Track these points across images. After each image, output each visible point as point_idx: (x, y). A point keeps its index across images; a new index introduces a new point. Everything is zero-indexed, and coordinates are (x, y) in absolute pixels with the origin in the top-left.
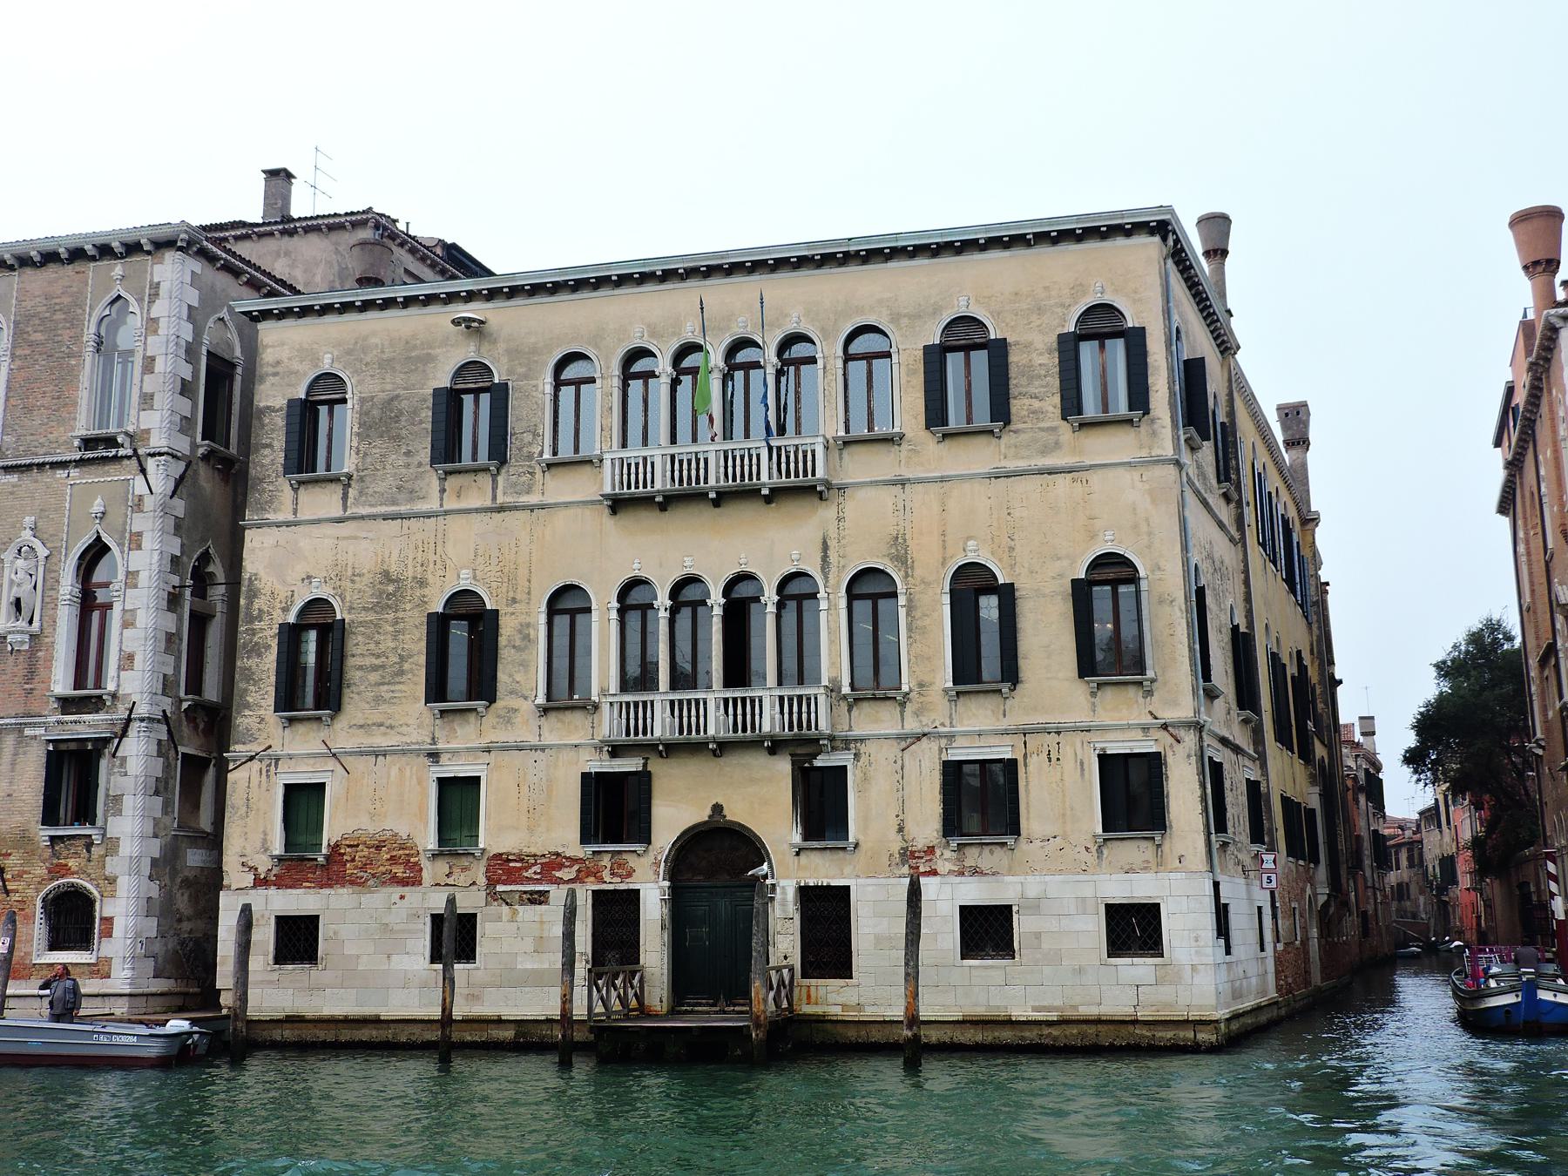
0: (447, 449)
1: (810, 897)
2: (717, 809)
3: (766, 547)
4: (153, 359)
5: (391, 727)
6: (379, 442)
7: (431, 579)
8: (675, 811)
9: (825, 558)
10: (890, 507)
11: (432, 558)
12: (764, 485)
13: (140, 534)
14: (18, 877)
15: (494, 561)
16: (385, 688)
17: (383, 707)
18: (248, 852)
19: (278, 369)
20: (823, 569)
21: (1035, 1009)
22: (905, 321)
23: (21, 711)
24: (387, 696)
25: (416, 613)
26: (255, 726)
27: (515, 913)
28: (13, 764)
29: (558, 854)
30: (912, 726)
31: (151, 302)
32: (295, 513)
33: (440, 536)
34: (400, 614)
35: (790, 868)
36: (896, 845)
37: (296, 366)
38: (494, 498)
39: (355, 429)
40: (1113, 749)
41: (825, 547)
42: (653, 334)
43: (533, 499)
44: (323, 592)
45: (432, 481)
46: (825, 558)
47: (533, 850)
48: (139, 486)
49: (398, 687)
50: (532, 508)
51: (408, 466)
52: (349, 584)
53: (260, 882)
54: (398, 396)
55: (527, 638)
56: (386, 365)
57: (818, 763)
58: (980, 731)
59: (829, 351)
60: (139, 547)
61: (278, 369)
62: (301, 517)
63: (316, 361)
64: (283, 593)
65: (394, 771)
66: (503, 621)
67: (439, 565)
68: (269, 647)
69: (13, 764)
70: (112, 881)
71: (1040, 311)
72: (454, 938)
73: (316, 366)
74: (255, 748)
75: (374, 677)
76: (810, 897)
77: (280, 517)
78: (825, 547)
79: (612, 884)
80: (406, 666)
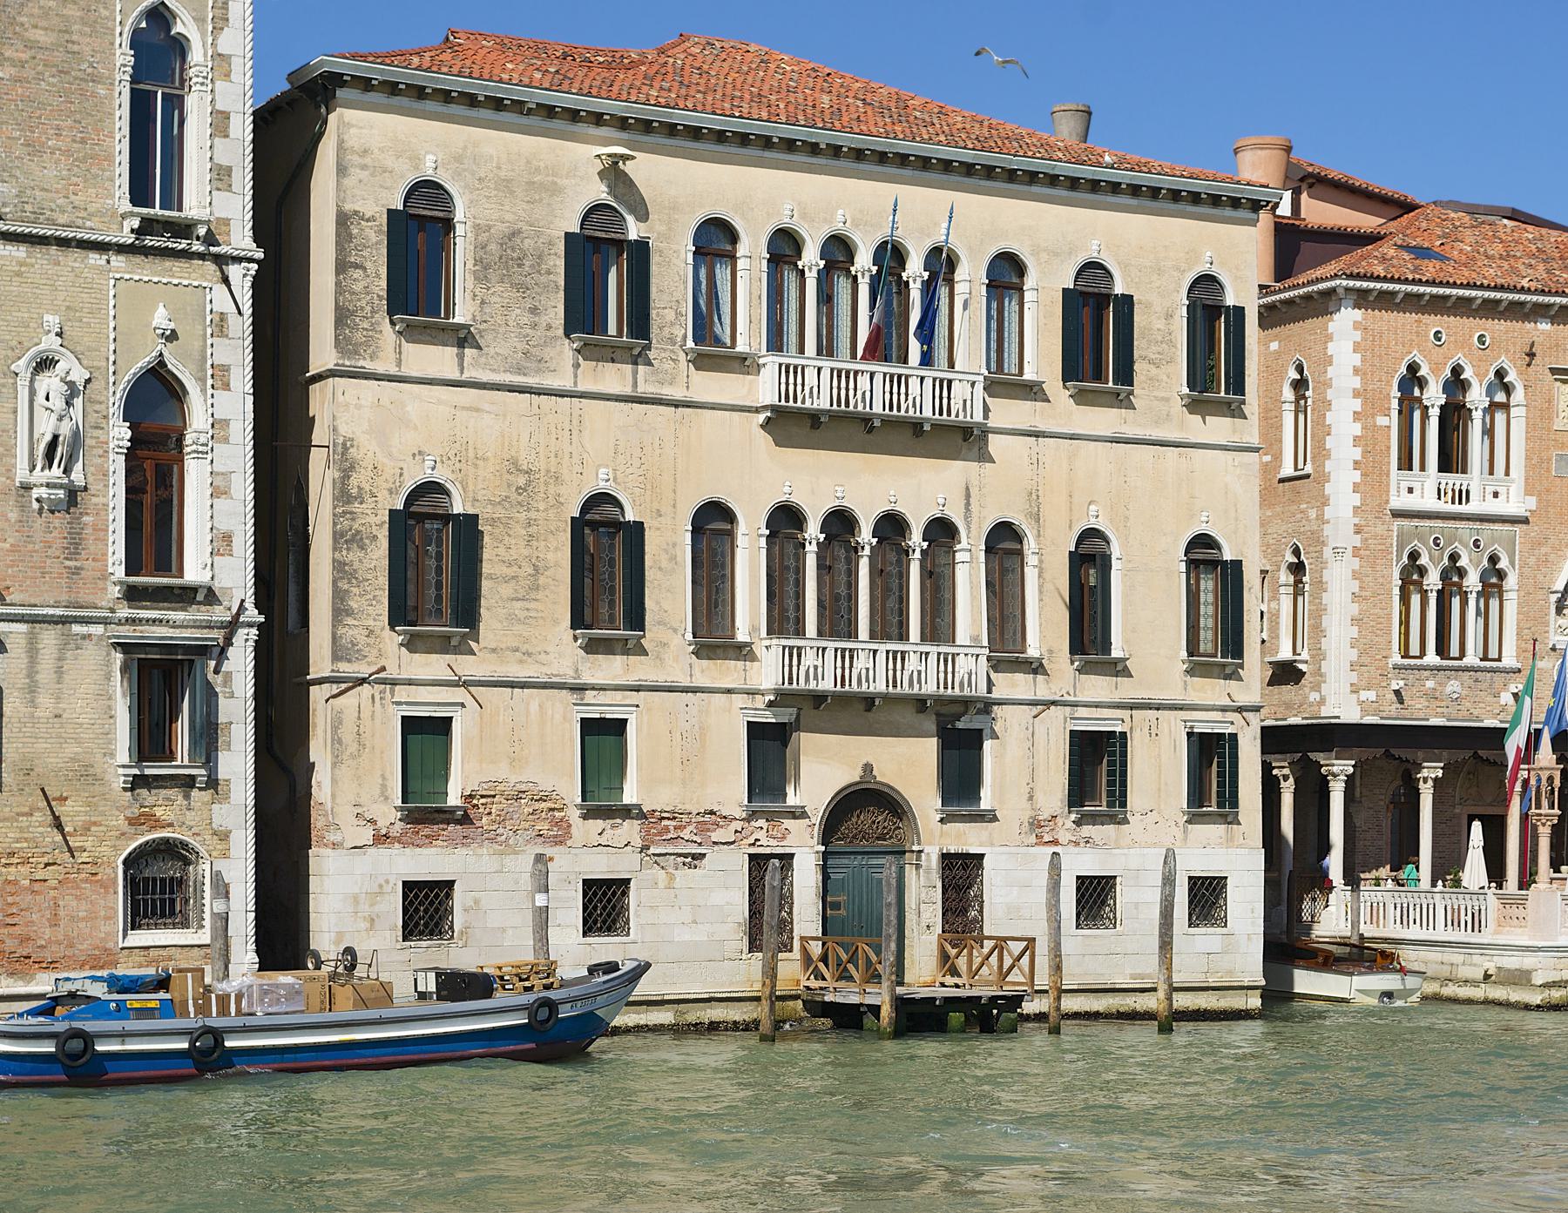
0: (583, 315)
1: (949, 861)
2: (868, 768)
3: (918, 488)
4: (226, 116)
5: (529, 654)
6: (498, 288)
7: (566, 475)
8: (824, 768)
9: (968, 504)
10: (1027, 461)
11: (568, 449)
12: (928, 419)
13: (225, 369)
14: (86, 829)
15: (637, 463)
16: (519, 604)
17: (518, 628)
18: (361, 801)
19: (368, 160)
20: (966, 518)
21: (1133, 977)
22: (1044, 256)
23: (64, 598)
24: (522, 614)
25: (551, 514)
26: (362, 640)
27: (672, 878)
28: (59, 672)
29: (712, 813)
30: (1043, 693)
31: (217, 30)
32: (399, 364)
33: (575, 422)
34: (533, 515)
35: (936, 835)
36: (1026, 816)
37: (389, 162)
38: (635, 384)
39: (470, 265)
40: (1200, 729)
41: (968, 496)
42: (804, 216)
43: (678, 393)
44: (440, 476)
45: (566, 350)
46: (968, 504)
47: (688, 808)
48: (220, 295)
49: (532, 605)
50: (676, 404)
51: (534, 326)
52: (472, 470)
53: (381, 839)
54: (520, 232)
55: (673, 558)
56: (506, 186)
57: (960, 725)
58: (1095, 699)
59: (971, 277)
60: (227, 387)
61: (368, 160)
62: (407, 371)
63: (416, 160)
64: (390, 470)
65: (534, 707)
66: (649, 536)
67: (576, 459)
68: (375, 538)
69: (59, 672)
70: (224, 836)
71: (1160, 271)
72: (604, 904)
73: (417, 168)
74: (363, 670)
75: (507, 590)
76: (949, 861)
77: (379, 367)
78: (968, 496)
79: (769, 846)
80: (542, 580)
